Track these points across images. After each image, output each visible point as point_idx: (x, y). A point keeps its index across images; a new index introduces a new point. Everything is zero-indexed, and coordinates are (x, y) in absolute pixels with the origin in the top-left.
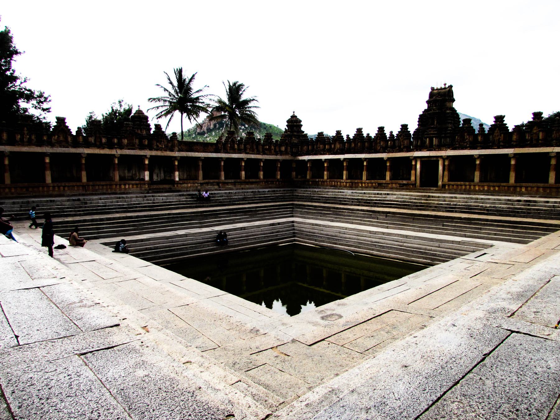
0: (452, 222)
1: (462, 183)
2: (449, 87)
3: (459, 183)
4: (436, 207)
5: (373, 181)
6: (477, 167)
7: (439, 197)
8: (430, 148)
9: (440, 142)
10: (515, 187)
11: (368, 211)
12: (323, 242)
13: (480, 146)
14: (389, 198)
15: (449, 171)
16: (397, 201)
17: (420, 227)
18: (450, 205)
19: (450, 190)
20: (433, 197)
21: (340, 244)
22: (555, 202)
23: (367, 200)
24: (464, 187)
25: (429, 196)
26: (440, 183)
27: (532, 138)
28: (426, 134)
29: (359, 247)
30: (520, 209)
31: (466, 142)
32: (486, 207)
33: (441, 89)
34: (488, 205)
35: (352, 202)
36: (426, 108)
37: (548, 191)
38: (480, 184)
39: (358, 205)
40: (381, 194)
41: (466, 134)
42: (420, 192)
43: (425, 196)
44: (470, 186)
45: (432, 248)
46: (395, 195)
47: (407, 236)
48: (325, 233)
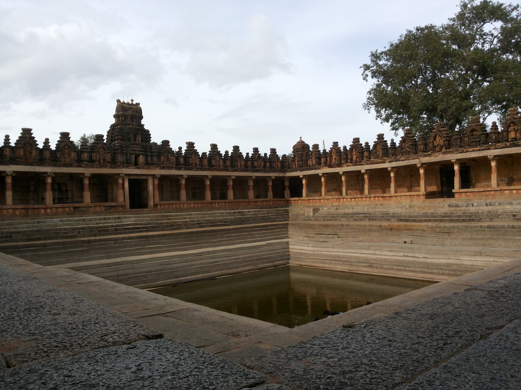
0: (228, 233)
1: (174, 202)
3: (171, 202)
5: (65, 205)
6: (183, 187)
7: (176, 216)
8: (136, 164)
9: (147, 160)
11: (138, 237)
12: (158, 280)
15: (159, 189)
17: (212, 242)
18: (194, 221)
20: (170, 216)
21: (183, 276)
23: (97, 228)
24: (174, 206)
26: (151, 203)
28: (132, 150)
29: (208, 272)
30: (241, 218)
31: (172, 163)
32: (221, 220)
33: (128, 104)
35: (79, 232)
38: (188, 202)
39: (95, 235)
40: (109, 219)
41: (170, 155)
42: (135, 214)
43: (163, 216)
44: (180, 204)
46: (129, 218)
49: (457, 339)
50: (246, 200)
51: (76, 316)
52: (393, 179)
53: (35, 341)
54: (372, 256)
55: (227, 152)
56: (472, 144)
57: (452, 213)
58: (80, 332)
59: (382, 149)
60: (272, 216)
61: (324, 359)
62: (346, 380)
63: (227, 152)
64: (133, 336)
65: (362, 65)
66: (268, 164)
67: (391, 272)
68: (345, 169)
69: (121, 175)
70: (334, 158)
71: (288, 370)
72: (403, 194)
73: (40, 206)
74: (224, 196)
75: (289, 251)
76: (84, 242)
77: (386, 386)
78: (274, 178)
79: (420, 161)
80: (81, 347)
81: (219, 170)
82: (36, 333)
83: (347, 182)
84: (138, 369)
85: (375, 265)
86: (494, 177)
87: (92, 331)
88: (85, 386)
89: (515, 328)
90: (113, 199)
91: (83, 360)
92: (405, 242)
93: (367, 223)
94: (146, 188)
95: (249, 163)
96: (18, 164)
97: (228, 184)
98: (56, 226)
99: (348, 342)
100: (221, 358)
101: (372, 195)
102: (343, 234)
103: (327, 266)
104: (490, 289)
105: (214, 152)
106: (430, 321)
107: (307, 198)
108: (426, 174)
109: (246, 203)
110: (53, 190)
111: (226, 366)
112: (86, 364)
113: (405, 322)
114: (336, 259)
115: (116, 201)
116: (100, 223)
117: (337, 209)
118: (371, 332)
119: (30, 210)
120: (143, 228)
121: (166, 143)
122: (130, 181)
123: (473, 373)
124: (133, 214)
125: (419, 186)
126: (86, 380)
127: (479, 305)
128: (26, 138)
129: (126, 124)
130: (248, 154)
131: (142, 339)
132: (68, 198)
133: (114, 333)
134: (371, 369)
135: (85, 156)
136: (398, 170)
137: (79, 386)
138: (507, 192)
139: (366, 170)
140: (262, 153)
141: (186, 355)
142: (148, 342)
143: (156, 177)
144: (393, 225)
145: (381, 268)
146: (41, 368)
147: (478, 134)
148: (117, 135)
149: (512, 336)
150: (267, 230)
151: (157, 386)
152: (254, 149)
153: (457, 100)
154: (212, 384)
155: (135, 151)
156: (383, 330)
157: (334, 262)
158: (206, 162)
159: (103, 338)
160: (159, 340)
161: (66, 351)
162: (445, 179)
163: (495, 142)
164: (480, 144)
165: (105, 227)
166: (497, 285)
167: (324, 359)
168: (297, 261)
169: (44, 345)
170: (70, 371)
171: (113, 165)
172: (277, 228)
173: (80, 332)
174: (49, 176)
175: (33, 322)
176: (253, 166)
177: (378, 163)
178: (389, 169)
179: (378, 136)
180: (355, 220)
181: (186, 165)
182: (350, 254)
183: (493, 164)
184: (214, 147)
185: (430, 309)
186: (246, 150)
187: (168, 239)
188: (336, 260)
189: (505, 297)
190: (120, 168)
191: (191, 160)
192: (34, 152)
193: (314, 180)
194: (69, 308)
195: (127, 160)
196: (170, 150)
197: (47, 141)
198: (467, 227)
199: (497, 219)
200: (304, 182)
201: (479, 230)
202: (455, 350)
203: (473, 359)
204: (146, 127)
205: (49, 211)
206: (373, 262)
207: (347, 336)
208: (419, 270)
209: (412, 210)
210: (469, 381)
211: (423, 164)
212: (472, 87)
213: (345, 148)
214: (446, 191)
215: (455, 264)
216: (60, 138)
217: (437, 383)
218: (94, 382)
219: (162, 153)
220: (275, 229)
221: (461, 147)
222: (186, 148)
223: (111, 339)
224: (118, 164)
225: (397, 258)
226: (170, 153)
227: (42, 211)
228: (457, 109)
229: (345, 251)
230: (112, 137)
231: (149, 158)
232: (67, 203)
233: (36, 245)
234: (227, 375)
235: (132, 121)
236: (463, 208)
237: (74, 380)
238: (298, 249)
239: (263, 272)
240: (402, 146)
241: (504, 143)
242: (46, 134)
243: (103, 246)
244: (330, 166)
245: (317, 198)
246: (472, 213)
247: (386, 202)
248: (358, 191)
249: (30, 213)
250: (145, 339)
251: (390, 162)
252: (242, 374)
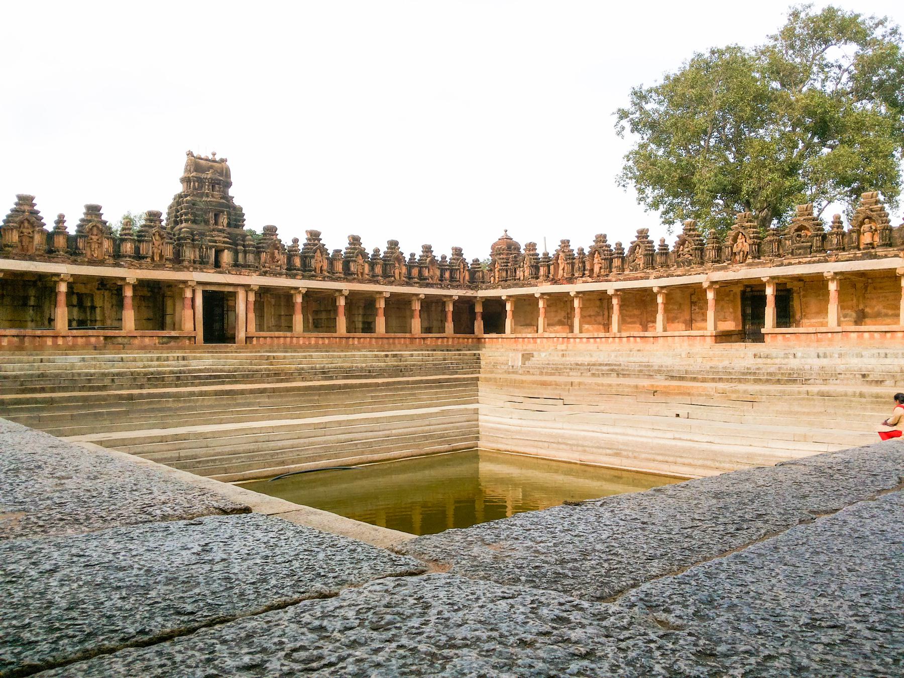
0: (376, 391)
1: (281, 334)
3: (277, 334)
5: (90, 332)
6: (298, 308)
7: (285, 358)
11: (216, 393)
12: (250, 467)
13: (303, 275)
14: (195, 365)
16: (222, 371)
17: (346, 406)
19: (261, 346)
21: (293, 463)
23: (145, 374)
25: (268, 358)
26: (241, 335)
28: (210, 241)
29: (336, 456)
32: (362, 368)
33: (207, 160)
34: (364, 365)
35: (113, 380)
38: (307, 335)
39: (141, 387)
41: (276, 251)
42: (212, 352)
46: (201, 358)
47: (377, 420)
48: (228, 449)
49: (760, 524)
50: (408, 335)
51: (99, 481)
52: (660, 308)
53: (24, 513)
54: (620, 438)
55: (377, 251)
56: (798, 252)
57: (758, 369)
58: (104, 501)
59: (645, 255)
60: (452, 363)
61: (530, 543)
62: (566, 571)
63: (377, 251)
64: (198, 508)
65: (615, 110)
66: (447, 275)
67: (652, 465)
68: (581, 286)
69: (190, 283)
70: (561, 268)
71: (466, 557)
72: (677, 333)
73: (46, 333)
74: (368, 327)
75: (478, 426)
76: (120, 397)
77: (634, 579)
78: (457, 298)
79: (708, 278)
80: (105, 521)
81: (361, 281)
82: (26, 502)
83: (582, 309)
84: (203, 550)
85: (625, 453)
86: (833, 307)
87: (126, 500)
88: (108, 568)
89: (858, 511)
90: (174, 325)
91: (106, 536)
92: (678, 415)
93: (613, 380)
94: (234, 309)
95: (415, 272)
96: (7, 257)
97: (378, 306)
98: (73, 367)
99: (573, 523)
100: (350, 539)
101: (624, 334)
102: (573, 398)
103: (543, 453)
104: (819, 464)
105: (355, 249)
106: (714, 501)
107: (513, 336)
108: (717, 300)
109: (408, 341)
110: (69, 305)
111: (359, 549)
112: (112, 541)
113: (670, 500)
114: (560, 441)
115: (180, 329)
116: (150, 366)
117: (563, 355)
118: (612, 511)
119: (26, 339)
120: (227, 377)
121: (271, 231)
123: (785, 565)
124: (209, 352)
125: (705, 320)
126: (110, 561)
127: (799, 484)
128: (24, 212)
129: (202, 195)
130: (413, 255)
131: (212, 513)
132: (96, 321)
133: (164, 503)
134: (610, 557)
135: (128, 247)
136: (670, 292)
137: (97, 568)
138: (853, 335)
139: (617, 290)
140: (438, 254)
141: (290, 534)
142: (224, 518)
143: (252, 290)
144: (657, 386)
145: (635, 458)
146: (30, 544)
147: (809, 234)
148: (186, 214)
149: (853, 521)
150: (442, 387)
151: (236, 571)
152: (423, 247)
153: (776, 175)
154: (333, 571)
155: (215, 242)
156: (632, 509)
157: (554, 445)
158: (339, 266)
159: (145, 510)
160: (243, 515)
161: (77, 526)
162: (749, 311)
163: (837, 249)
164: (811, 253)
165: (159, 373)
166: (830, 460)
167: (530, 543)
168: (493, 442)
169: (39, 518)
170: (82, 550)
171: (176, 266)
172: (460, 385)
173: (104, 501)
174: (62, 280)
175: (21, 487)
176: (421, 277)
177: (636, 279)
178: (655, 290)
179: (638, 232)
180: (593, 375)
181: (305, 271)
182: (583, 433)
183: (833, 287)
184: (355, 241)
185: (715, 486)
186: (410, 249)
187: (269, 397)
188: (558, 443)
189: (843, 475)
190: (188, 268)
191: (313, 261)
192: (37, 238)
193: (526, 305)
194: (87, 470)
196: (277, 246)
197: (61, 220)
198: (783, 393)
199: (835, 382)
200: (508, 307)
201: (803, 399)
202: (754, 538)
203: (786, 549)
204: (237, 202)
205: (60, 341)
206: (621, 447)
207: (570, 515)
208: (700, 462)
209: (691, 361)
210: (778, 574)
211: (713, 283)
212: (802, 156)
213: (581, 251)
214: (750, 331)
215: (760, 455)
216: (85, 214)
217: (723, 576)
218: (123, 564)
219: (263, 247)
220: (456, 386)
221: (779, 256)
222: (306, 241)
223: (158, 512)
224: (186, 263)
225: (662, 442)
226: (277, 248)
227: (49, 342)
228: (775, 192)
229: (575, 427)
230: (176, 217)
231: (240, 256)
232: (94, 329)
233: (36, 401)
234: (359, 561)
236: (777, 361)
237: (88, 561)
238: (494, 423)
239: (430, 460)
240: (678, 251)
241: (853, 251)
242: (61, 209)
243: (154, 406)
244: (555, 282)
245: (529, 336)
246: (793, 369)
247: (649, 346)
248: (602, 326)
249: (26, 344)
250: (218, 514)
251: (656, 278)
252: (385, 560)
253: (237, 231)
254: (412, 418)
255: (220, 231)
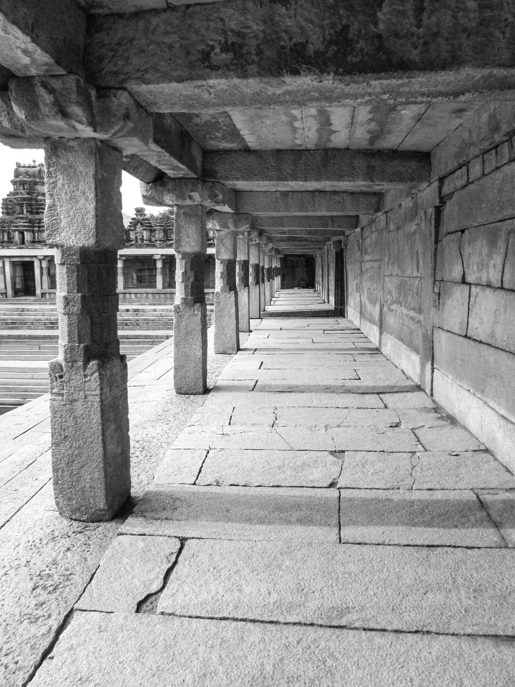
0: (51, 342)
2: (39, 165)
4: (32, 323)
7: (36, 310)
9: (34, 238)
10: (124, 293)
17: (8, 353)
22: (163, 310)
25: (23, 310)
26: (38, 291)
27: (136, 237)
28: (14, 226)
33: (29, 167)
36: (12, 190)
37: (157, 297)
42: (12, 304)
45: (25, 381)
81: (140, 247)
122: (14, 264)
124: (10, 304)
155: (17, 227)
195: (9, 238)
235: (24, 189)
253: (37, 217)
254: (23, 370)
255: (21, 218)
